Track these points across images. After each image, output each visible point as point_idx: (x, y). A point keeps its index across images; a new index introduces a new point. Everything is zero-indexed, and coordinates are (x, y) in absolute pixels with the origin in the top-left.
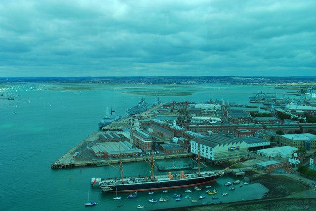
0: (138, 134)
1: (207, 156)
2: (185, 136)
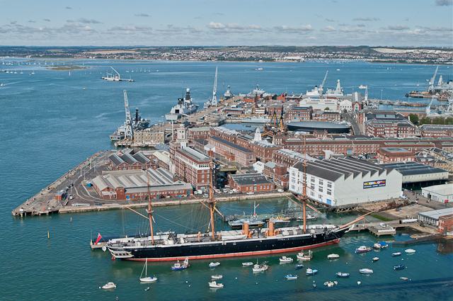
0: (184, 154)
1: (320, 197)
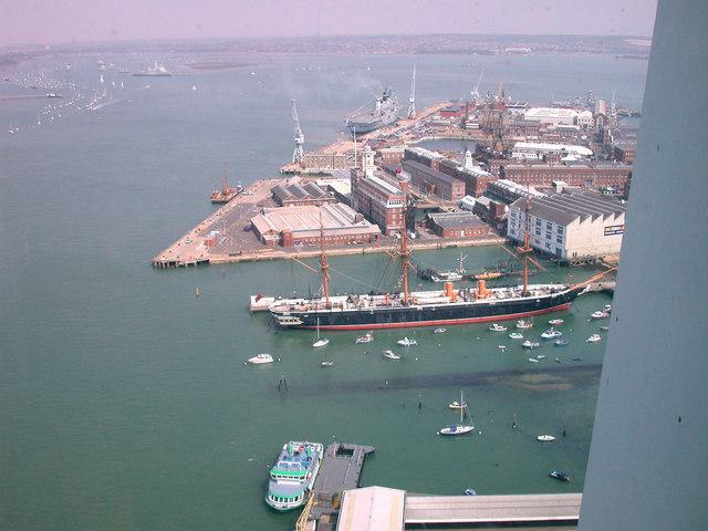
1: (548, 245)
2: (493, 191)
